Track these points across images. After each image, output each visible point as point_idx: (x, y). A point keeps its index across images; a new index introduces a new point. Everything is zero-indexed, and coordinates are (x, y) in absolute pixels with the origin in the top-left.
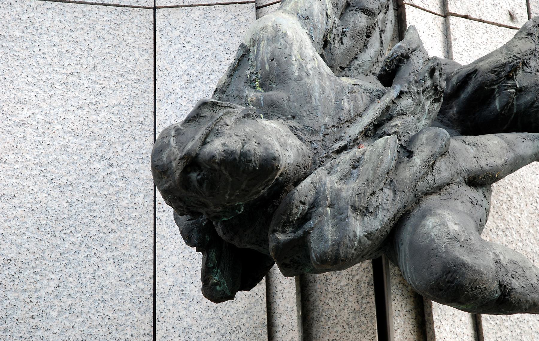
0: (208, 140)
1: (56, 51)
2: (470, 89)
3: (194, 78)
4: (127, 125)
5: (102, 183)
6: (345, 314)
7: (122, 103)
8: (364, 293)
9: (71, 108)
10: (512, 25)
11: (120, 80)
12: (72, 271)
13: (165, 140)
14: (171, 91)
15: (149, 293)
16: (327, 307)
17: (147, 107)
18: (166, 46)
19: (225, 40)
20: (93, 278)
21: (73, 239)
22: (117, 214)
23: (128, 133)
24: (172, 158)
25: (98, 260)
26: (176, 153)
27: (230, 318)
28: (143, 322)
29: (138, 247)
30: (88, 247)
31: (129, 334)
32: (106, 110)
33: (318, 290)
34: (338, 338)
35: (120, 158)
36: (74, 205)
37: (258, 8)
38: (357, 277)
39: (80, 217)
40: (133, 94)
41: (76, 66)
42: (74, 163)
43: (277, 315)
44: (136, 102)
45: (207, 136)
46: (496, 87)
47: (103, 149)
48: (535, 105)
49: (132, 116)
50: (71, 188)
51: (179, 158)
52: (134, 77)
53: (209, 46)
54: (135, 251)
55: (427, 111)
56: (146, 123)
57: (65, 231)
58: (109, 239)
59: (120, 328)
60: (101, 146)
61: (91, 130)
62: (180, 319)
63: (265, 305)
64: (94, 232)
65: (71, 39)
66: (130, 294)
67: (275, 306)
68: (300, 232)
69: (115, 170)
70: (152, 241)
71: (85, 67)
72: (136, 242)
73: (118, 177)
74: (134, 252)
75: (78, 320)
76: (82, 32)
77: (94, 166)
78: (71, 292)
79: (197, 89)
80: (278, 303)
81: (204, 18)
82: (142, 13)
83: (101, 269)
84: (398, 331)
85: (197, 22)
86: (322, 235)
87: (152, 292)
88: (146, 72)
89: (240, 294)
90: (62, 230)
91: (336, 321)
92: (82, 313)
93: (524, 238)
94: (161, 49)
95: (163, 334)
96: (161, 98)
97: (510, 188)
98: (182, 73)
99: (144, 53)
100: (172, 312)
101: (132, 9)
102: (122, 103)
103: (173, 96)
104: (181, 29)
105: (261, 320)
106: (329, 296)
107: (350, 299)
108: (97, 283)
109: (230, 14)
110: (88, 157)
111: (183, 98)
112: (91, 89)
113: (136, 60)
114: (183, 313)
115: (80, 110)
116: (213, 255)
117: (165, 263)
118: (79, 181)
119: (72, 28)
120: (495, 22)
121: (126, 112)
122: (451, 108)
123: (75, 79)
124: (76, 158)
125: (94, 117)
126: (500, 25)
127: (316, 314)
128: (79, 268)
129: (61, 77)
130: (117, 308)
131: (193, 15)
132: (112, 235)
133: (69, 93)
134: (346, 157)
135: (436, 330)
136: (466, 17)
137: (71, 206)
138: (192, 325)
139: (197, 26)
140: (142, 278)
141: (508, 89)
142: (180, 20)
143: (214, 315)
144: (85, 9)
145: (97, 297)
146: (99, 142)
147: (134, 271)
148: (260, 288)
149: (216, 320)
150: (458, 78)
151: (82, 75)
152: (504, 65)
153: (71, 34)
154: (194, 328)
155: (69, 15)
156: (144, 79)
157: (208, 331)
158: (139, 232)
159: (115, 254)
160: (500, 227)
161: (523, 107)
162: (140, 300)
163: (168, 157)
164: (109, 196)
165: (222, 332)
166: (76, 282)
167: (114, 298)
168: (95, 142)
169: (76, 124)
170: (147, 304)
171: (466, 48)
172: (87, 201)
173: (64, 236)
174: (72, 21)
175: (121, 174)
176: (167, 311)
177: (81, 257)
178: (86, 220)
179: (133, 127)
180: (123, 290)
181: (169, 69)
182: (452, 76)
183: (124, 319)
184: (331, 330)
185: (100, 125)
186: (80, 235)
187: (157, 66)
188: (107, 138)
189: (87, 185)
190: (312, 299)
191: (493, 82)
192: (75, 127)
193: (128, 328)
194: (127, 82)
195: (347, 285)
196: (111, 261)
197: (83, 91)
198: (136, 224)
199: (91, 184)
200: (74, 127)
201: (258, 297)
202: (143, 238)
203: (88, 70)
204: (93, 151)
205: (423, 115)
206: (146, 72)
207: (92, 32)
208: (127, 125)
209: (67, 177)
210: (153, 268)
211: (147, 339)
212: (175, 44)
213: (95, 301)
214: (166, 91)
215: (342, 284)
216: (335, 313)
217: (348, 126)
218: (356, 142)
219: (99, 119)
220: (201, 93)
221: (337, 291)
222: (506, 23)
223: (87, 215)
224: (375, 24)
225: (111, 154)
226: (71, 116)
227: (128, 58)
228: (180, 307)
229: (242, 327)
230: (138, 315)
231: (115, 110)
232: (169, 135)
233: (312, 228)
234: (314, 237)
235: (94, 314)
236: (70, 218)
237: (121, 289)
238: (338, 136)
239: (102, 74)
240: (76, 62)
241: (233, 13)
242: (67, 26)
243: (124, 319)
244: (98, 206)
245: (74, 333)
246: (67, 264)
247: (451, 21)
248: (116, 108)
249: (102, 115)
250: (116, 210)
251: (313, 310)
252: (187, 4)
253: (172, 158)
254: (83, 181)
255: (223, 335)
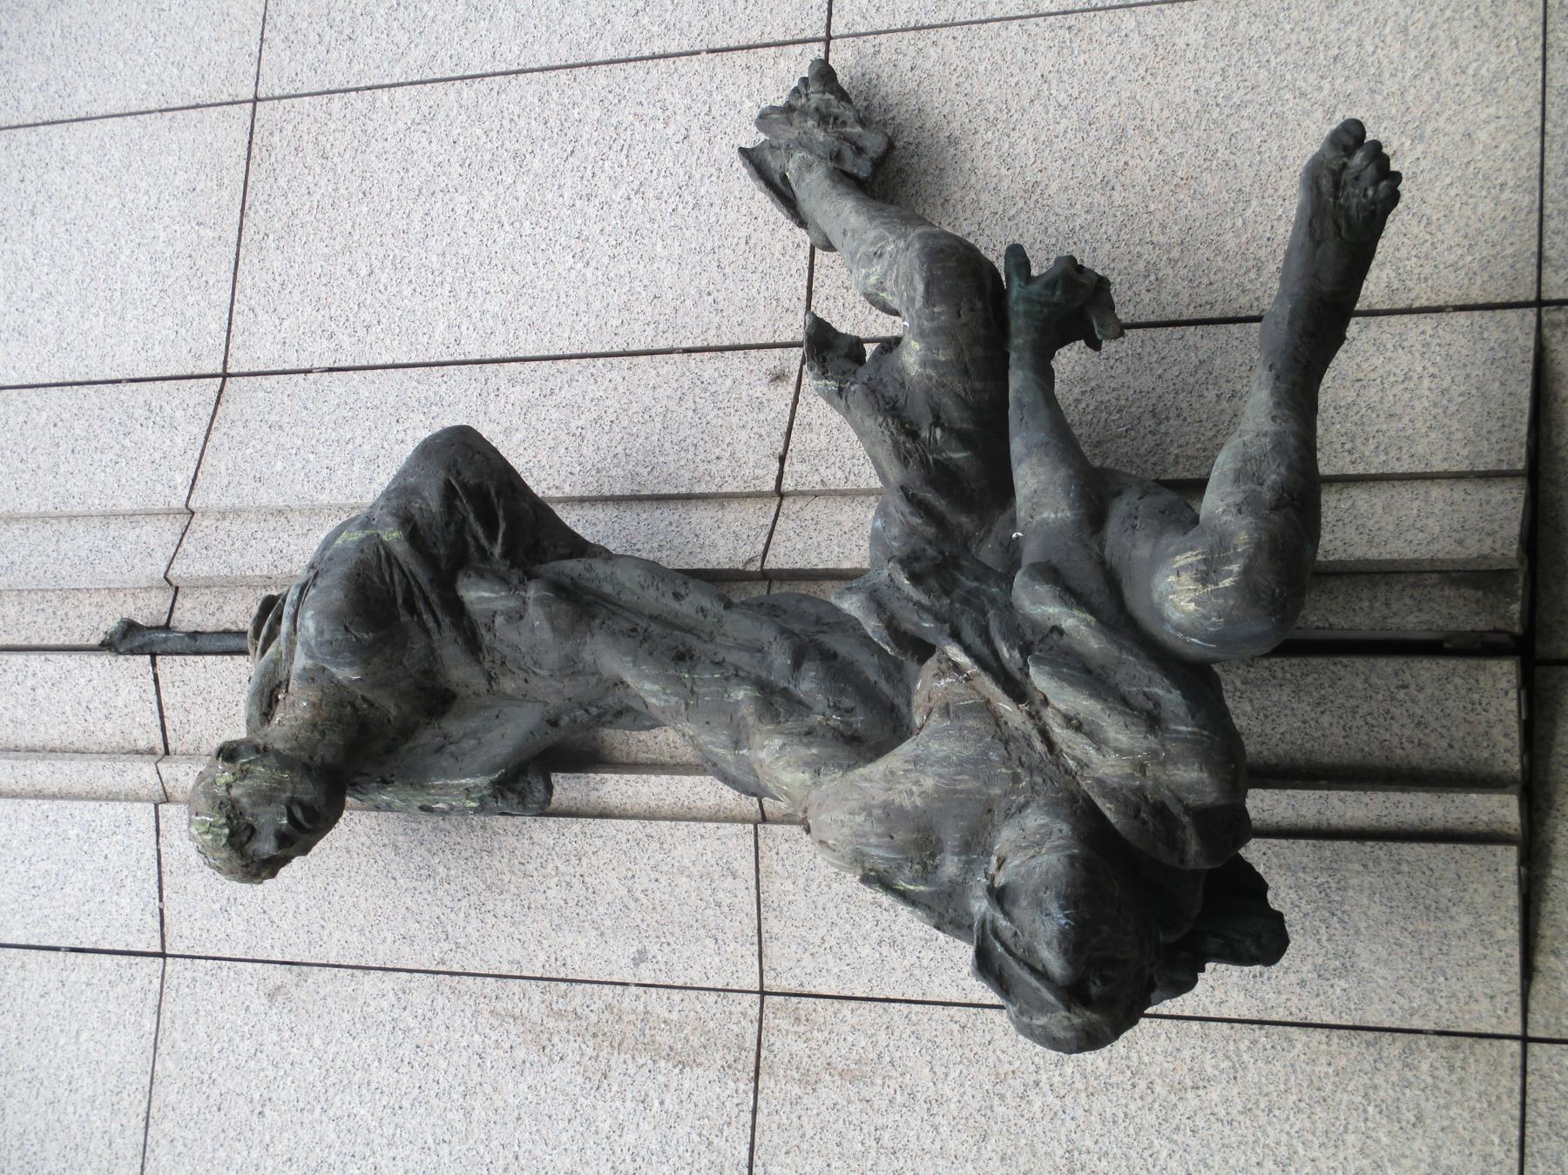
0: (1039, 967)
1: (839, 1164)
2: (930, 496)
3: (887, 934)
4: (967, 1051)
5: (1068, 1100)
6: (1303, 707)
7: (929, 1058)
8: (1266, 674)
9: (938, 1145)
10: (794, 379)
11: (888, 1059)
12: (1217, 1158)
13: (1037, 1032)
14: (907, 974)
15: (1259, 1033)
16: (1288, 736)
17: (936, 1017)
18: (830, 978)
19: (821, 879)
20: (1230, 1123)
21: (1164, 1154)
22: (1121, 1078)
23: (980, 1052)
24: (1066, 1023)
25: (1200, 1113)
26: (1059, 1017)
27: (1304, 902)
28: (1307, 1045)
29: (1178, 1046)
30: (1178, 1128)
31: (1325, 1068)
32: (940, 1085)
33: (1259, 748)
34: (1342, 722)
35: (1024, 1066)
36: (1104, 1149)
37: (764, 819)
38: (1238, 683)
39: (1126, 1140)
40: (913, 1039)
41: (865, 1131)
42: (1032, 1145)
43: (1300, 822)
44: (927, 1035)
45: (1033, 970)
46: (930, 457)
47: (1008, 1095)
48: (963, 394)
49: (950, 1043)
50: (1076, 1154)
51: (1067, 1014)
52: (882, 1036)
53: (830, 905)
54: (1184, 1052)
55: (975, 584)
56: (963, 1020)
57: (1150, 1166)
58: (1164, 1093)
59: (1316, 1083)
60: (1002, 1097)
61: (975, 1113)
62: (1302, 984)
63: (1284, 841)
64: (1151, 1118)
65: (817, 1138)
66: (1260, 1063)
67: (1285, 824)
68: (1186, 819)
69: (1044, 1077)
70: (1167, 1022)
71: (865, 1118)
72: (1170, 1049)
73: (1057, 1073)
74: (1186, 1053)
75: (1301, 1152)
76: (805, 1119)
77: (1038, 1111)
78: (1254, 1160)
79: (905, 932)
80: (1279, 818)
81: (781, 912)
82: (771, 1016)
83: (1216, 1110)
84: (1332, 620)
85: (789, 924)
86: (1190, 788)
87: (1255, 1026)
88: (873, 1015)
89: (1275, 901)
90: (1148, 1170)
91: (1313, 723)
92: (1290, 1146)
93: (1172, 387)
94: (833, 986)
95: (1328, 1013)
96: (920, 992)
97: (1083, 405)
98: (877, 955)
99: (840, 1016)
100: (1290, 996)
101: (764, 1032)
102: (929, 1058)
103: (917, 972)
104: (799, 951)
105: (1308, 849)
106: (1268, 730)
107: (1275, 698)
108: (1240, 1118)
109: (776, 868)
110: (1022, 1122)
111: (921, 955)
112: (904, 1110)
113: (854, 1029)
114: (1293, 978)
115: (941, 1130)
116: (1213, 943)
117: (1207, 1002)
118: (1064, 1139)
119: (797, 1134)
120: (790, 407)
121: (944, 1052)
122: (960, 526)
123: (886, 1136)
124: (1023, 1141)
125: (953, 1106)
126: (796, 401)
127: (1299, 755)
128: (1213, 1145)
129: (883, 1158)
130: (1282, 1087)
131: (776, 930)
132: (1158, 1089)
133: (911, 1146)
134: (1059, 733)
135: (1331, 558)
136: (782, 460)
137: (1106, 1153)
138: (1314, 965)
139: (796, 923)
140: (1232, 1043)
141: (935, 438)
142: (785, 951)
143: (1298, 927)
144: (766, 1111)
145: (1263, 1119)
146: (996, 1101)
147: (1220, 1055)
148: (1255, 853)
149: (1307, 923)
150: (912, 514)
151: (880, 1121)
152: (896, 444)
153: (808, 1136)
154: (1320, 961)
155: (776, 1140)
156: (886, 1018)
157: (1324, 938)
158: (1151, 1044)
159: (1189, 1083)
160: (1152, 428)
161: (965, 415)
162: (1269, 1047)
163: (1064, 1029)
164: (1090, 1090)
165: (1327, 914)
166: (1238, 1153)
167: (1266, 1090)
168: (995, 1109)
169: (964, 1137)
170: (1276, 1037)
171: (838, 464)
172: (1098, 1126)
173: (1158, 1168)
174: (786, 1134)
175: (1053, 1067)
176: (1289, 1004)
177: (1193, 1142)
178: (1131, 1131)
179: (971, 1042)
180: (1252, 1075)
181: (870, 975)
182: (908, 523)
183: (1300, 1076)
184: (1327, 732)
185: (966, 1098)
186: (1156, 1142)
187: (864, 995)
188: (988, 1086)
189: (1071, 1125)
190: (1274, 760)
191: (924, 463)
192: (969, 1139)
193: (1317, 1069)
194: (891, 1048)
195: (1251, 701)
196: (1201, 1092)
197: (907, 1121)
198: (1138, 1047)
199: (1068, 1118)
200: (971, 1141)
201: (1269, 852)
202: (1163, 1037)
203: (870, 1113)
204: (1012, 1112)
205: (984, 592)
206: (873, 1015)
207: (805, 1101)
208: (967, 1051)
209: (1057, 1159)
210: (1214, 1024)
211: (1336, 1040)
212: (826, 963)
213: (1270, 1123)
214: (909, 982)
215: (1249, 709)
216: (1299, 724)
217: (1006, 723)
218: (1034, 716)
219: (955, 1099)
220: (912, 926)
221: (1261, 717)
222: (792, 389)
223: (1122, 1128)
224: (811, 641)
225: (1017, 1083)
226: (952, 1144)
227: (849, 1043)
228: (1283, 982)
229: (1319, 881)
230: (1296, 1052)
231: (940, 1071)
232: (1029, 1026)
233: (1180, 801)
234: (1192, 799)
235: (1292, 1126)
236: (1128, 1159)
237: (1249, 1078)
238: (1021, 740)
239: (878, 1089)
240: (857, 1132)
241: (774, 863)
242: (795, 1143)
243: (1300, 1076)
244: (1108, 1110)
245: (1323, 1160)
246: (1206, 1165)
247: (791, 489)
248: (936, 1069)
249: (948, 1092)
250: (1114, 1080)
251: (1292, 759)
252: (756, 939)
253: (1066, 1023)
254: (1063, 1131)
255: (1333, 915)
